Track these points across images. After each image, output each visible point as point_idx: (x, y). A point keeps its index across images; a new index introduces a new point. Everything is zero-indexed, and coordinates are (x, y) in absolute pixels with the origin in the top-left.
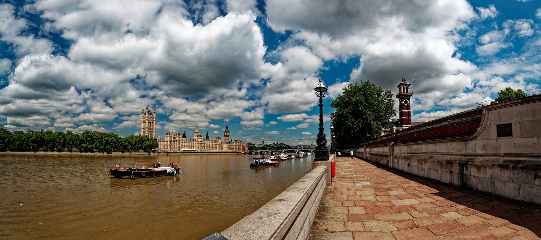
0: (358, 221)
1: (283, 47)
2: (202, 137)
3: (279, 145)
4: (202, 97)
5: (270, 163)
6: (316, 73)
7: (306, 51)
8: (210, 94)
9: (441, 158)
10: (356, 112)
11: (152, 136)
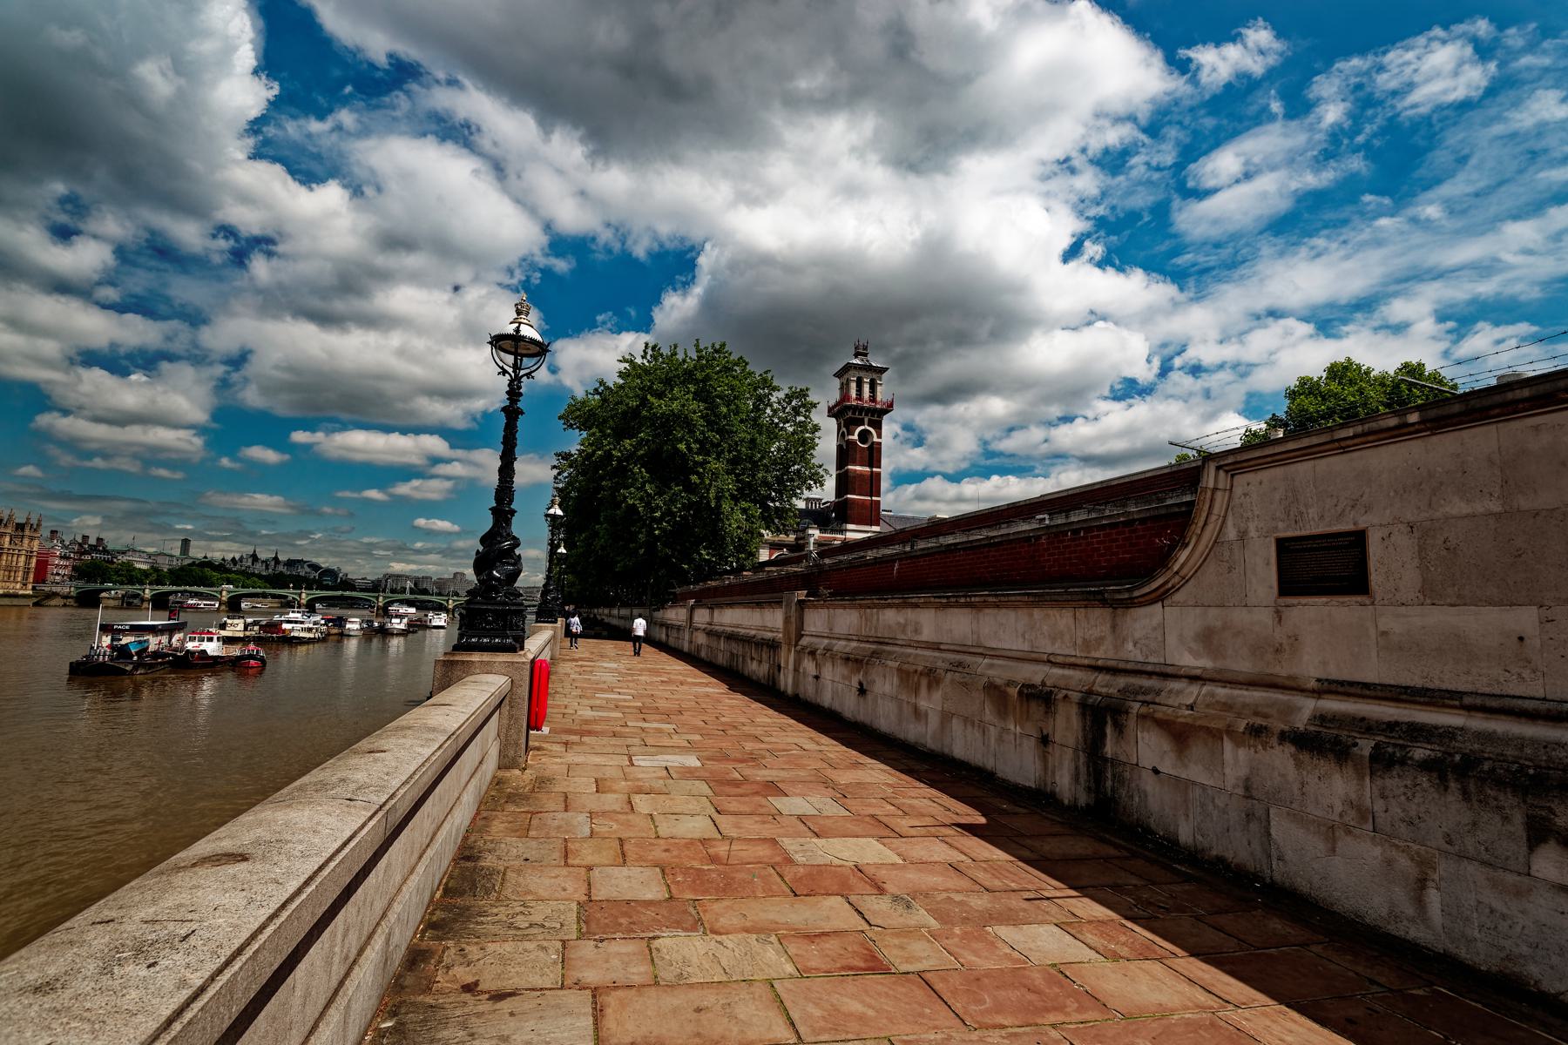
0: (629, 934)
3: (281, 568)
5: (210, 653)
6: (510, 272)
9: (1000, 672)
10: (664, 455)
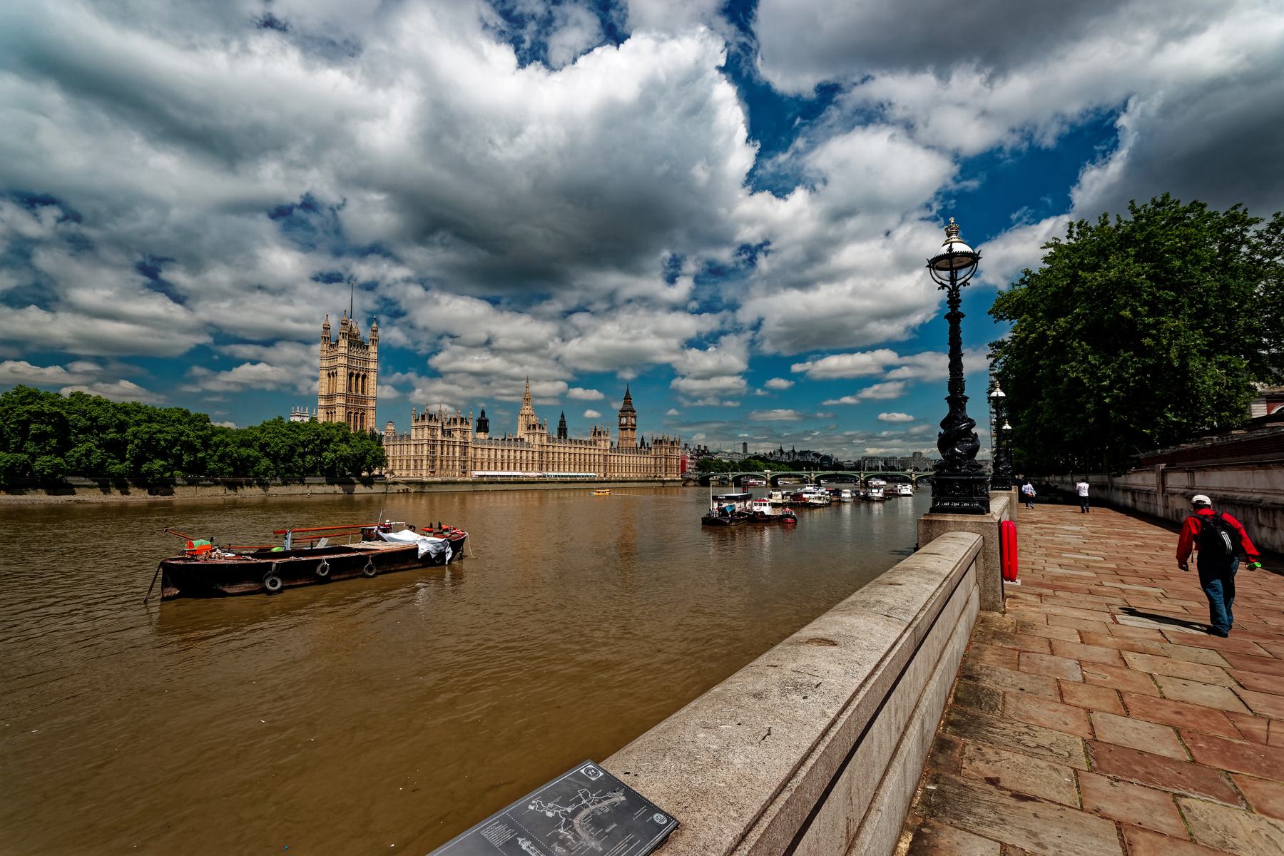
1: (812, 139)
2: (545, 432)
3: (797, 457)
4: (545, 297)
5: (766, 513)
7: (892, 137)
8: (572, 288)
10: (1105, 325)
11: (362, 427)
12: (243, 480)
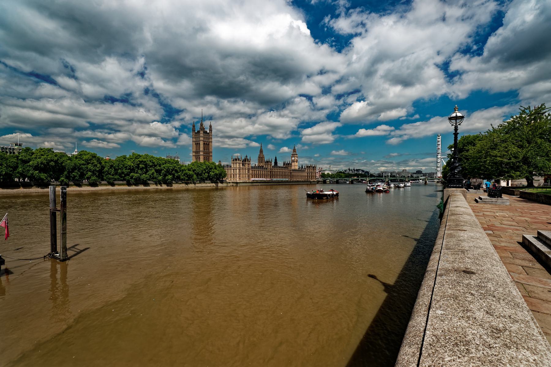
12: (189, 182)
